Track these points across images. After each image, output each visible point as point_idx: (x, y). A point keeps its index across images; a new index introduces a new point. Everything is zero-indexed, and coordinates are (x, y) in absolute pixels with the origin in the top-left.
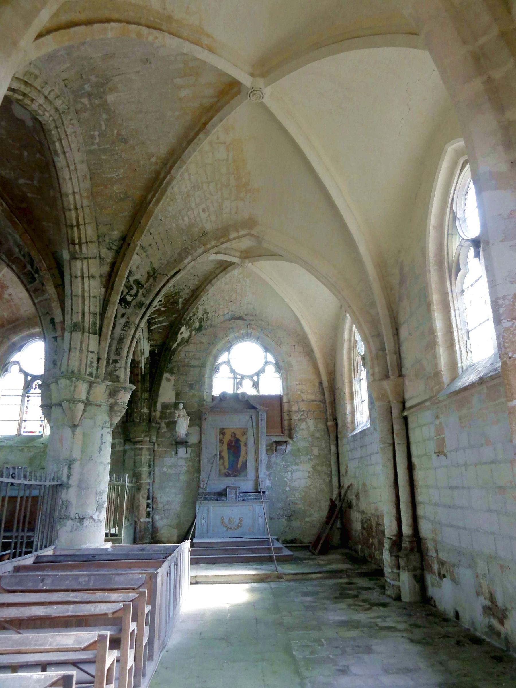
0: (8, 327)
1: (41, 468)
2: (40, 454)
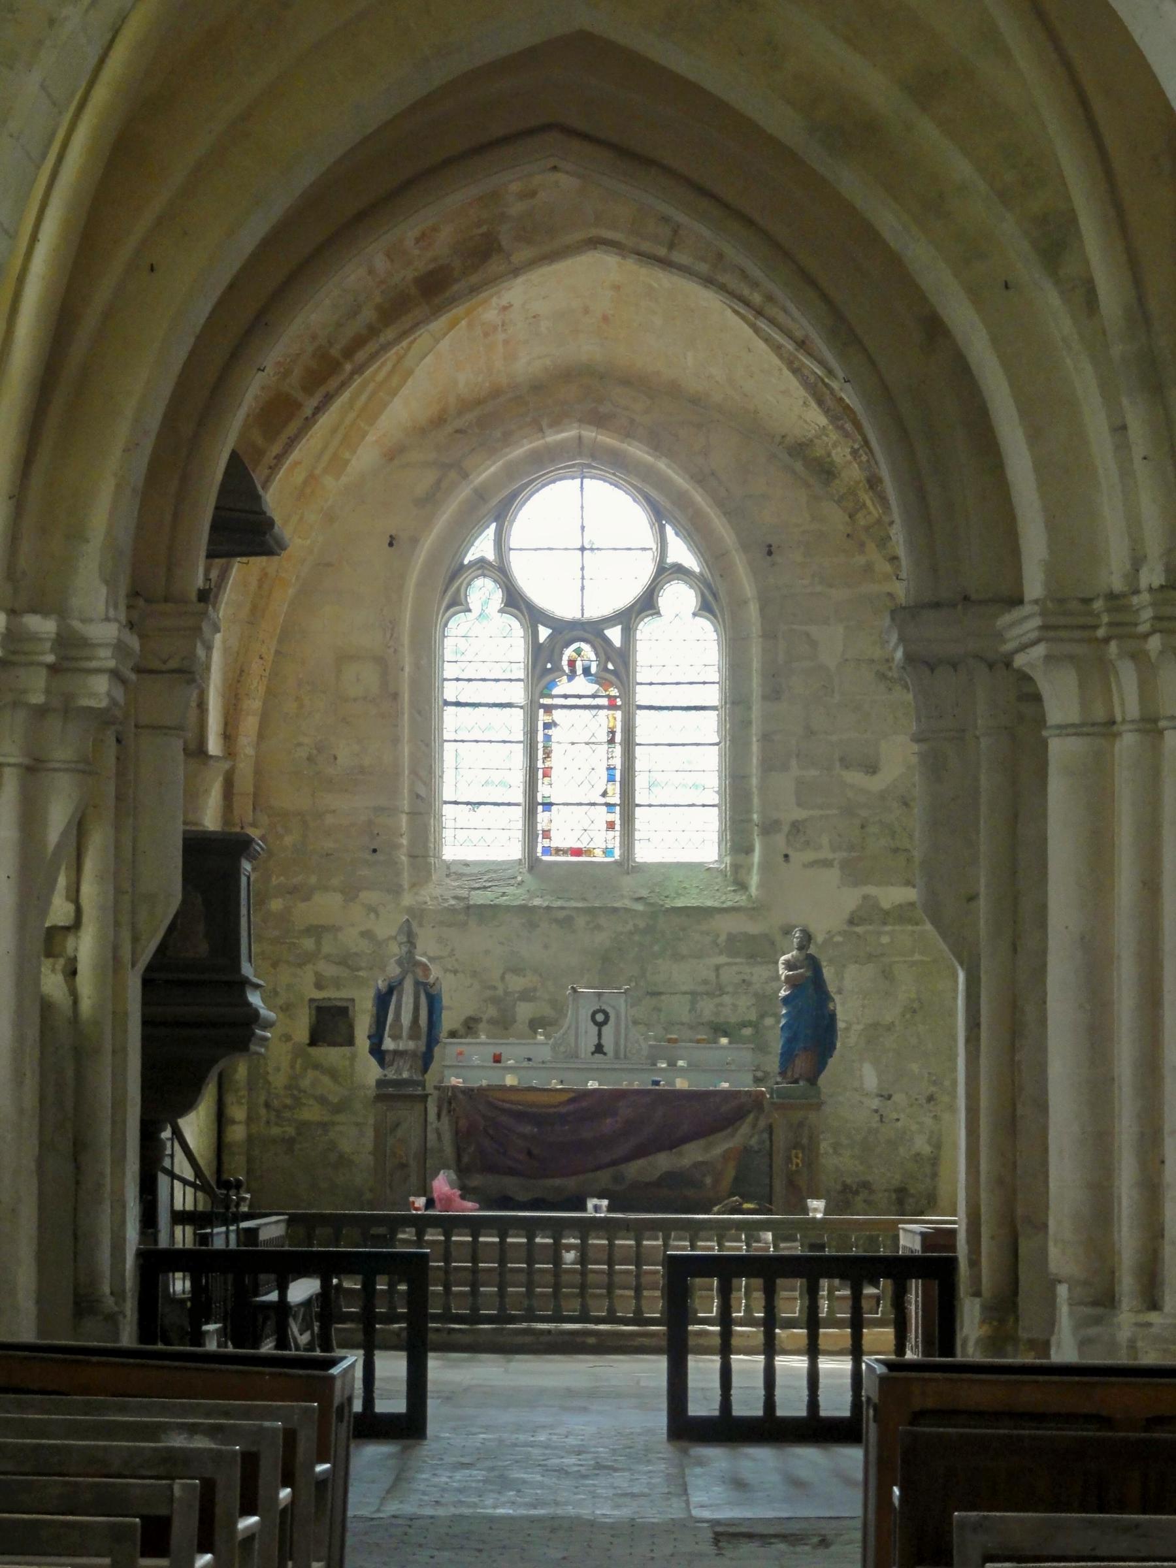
0: (459, 423)
2: (637, 938)
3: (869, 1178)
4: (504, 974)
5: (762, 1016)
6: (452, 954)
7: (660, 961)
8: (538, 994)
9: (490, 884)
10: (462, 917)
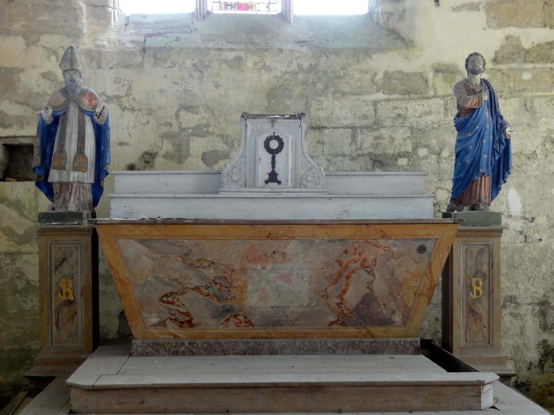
1: (313, 128)
2: (301, 76)
3: (515, 293)
4: (178, 111)
5: (415, 149)
6: (128, 93)
7: (322, 98)
8: (210, 129)
9: (164, 31)
10: (138, 59)
